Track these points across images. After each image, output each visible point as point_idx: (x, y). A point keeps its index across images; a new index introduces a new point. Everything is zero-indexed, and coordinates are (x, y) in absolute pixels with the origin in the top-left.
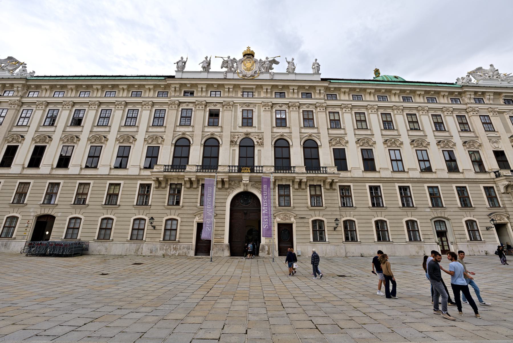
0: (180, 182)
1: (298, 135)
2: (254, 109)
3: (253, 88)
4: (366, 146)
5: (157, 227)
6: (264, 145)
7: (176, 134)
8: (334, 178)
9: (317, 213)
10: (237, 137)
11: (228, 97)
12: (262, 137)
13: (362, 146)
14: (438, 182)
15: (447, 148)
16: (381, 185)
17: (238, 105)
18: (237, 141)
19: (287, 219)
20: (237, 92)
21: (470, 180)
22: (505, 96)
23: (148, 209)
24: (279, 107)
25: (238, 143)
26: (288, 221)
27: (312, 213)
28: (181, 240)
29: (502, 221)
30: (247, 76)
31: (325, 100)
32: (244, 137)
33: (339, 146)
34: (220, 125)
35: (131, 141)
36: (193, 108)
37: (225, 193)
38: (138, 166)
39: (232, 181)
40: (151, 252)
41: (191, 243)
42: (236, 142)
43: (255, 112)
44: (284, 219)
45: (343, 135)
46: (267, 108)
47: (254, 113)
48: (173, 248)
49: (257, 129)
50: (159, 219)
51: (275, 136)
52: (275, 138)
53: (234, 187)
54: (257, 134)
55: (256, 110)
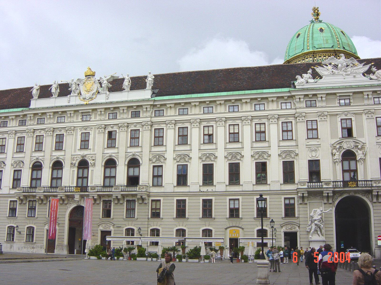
0: (35, 199)
1: (124, 154)
2: (90, 132)
3: (89, 112)
4: (182, 162)
5: (22, 233)
6: (96, 166)
7: (32, 159)
8: (142, 195)
9: (130, 223)
10: (75, 159)
11: (70, 122)
12: (94, 158)
13: (178, 162)
14: (242, 195)
15: (261, 160)
16: (187, 198)
17: (78, 128)
18: (75, 163)
19: (108, 228)
20: (77, 116)
21: (273, 192)
22: (340, 96)
23: (16, 219)
24: (111, 128)
25: (77, 165)
26: (108, 229)
27: (126, 223)
28: (37, 242)
29: (293, 230)
30: (87, 98)
31: (151, 117)
32: (81, 159)
33: (158, 163)
34: (63, 149)
35: (2, 166)
36: (44, 135)
37: (64, 207)
38: (8, 187)
39: (70, 198)
40: (19, 250)
41: (43, 244)
42: (75, 164)
43: (91, 134)
44: (105, 228)
45: (163, 152)
46: (101, 130)
47: (90, 135)
48: (32, 247)
49: (92, 150)
50: (23, 227)
51: (105, 156)
52: (105, 158)
53: (71, 203)
54: (91, 156)
55: (92, 133)
